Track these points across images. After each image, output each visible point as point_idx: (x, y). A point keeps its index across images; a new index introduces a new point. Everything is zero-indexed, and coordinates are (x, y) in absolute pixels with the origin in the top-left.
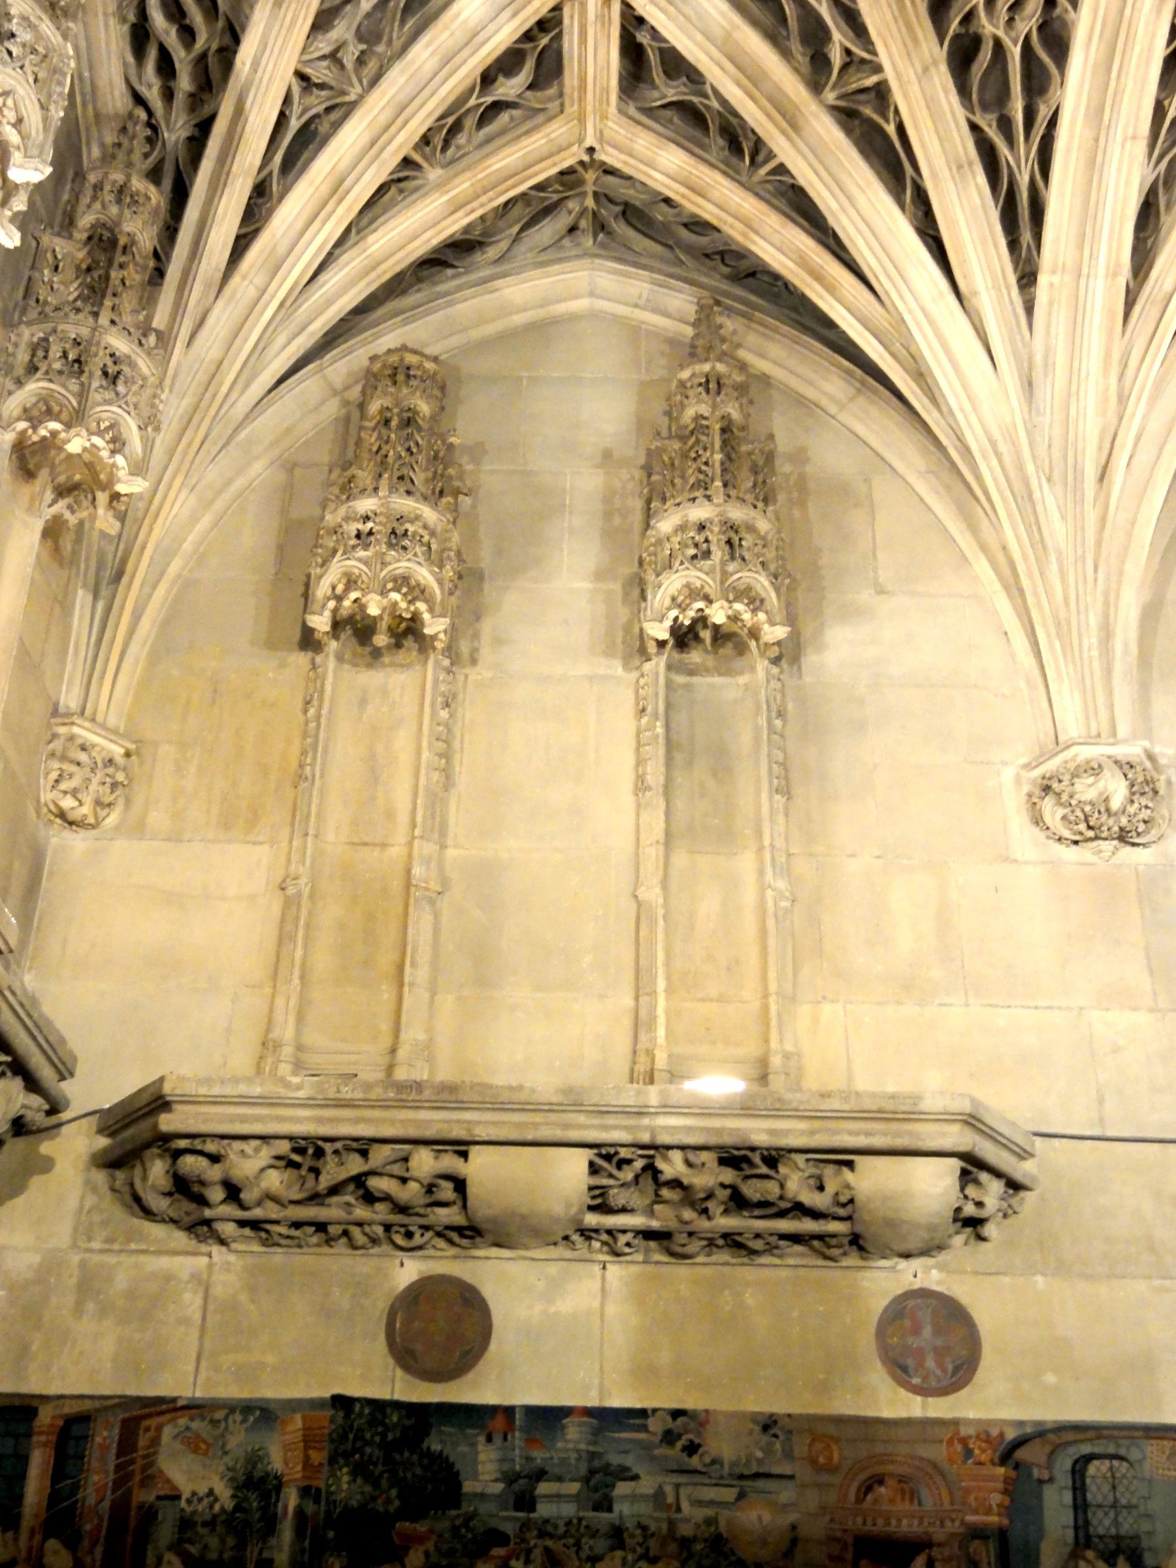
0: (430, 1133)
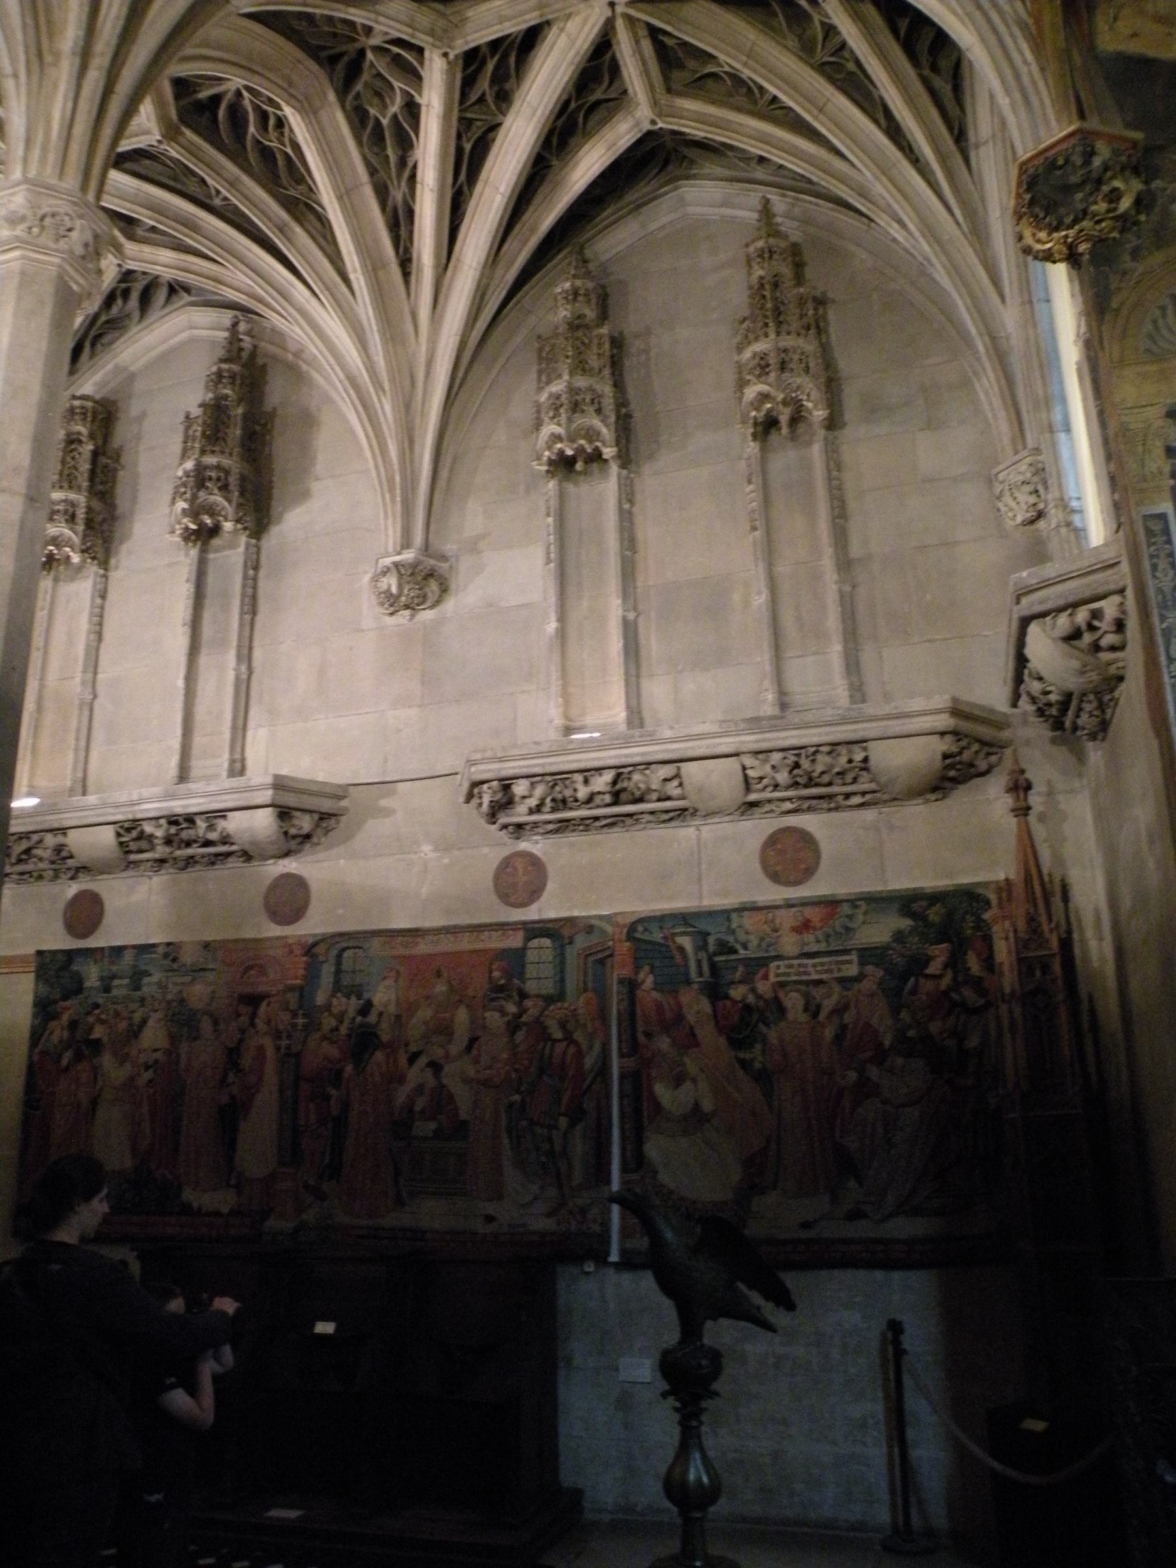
0: (46, 826)
